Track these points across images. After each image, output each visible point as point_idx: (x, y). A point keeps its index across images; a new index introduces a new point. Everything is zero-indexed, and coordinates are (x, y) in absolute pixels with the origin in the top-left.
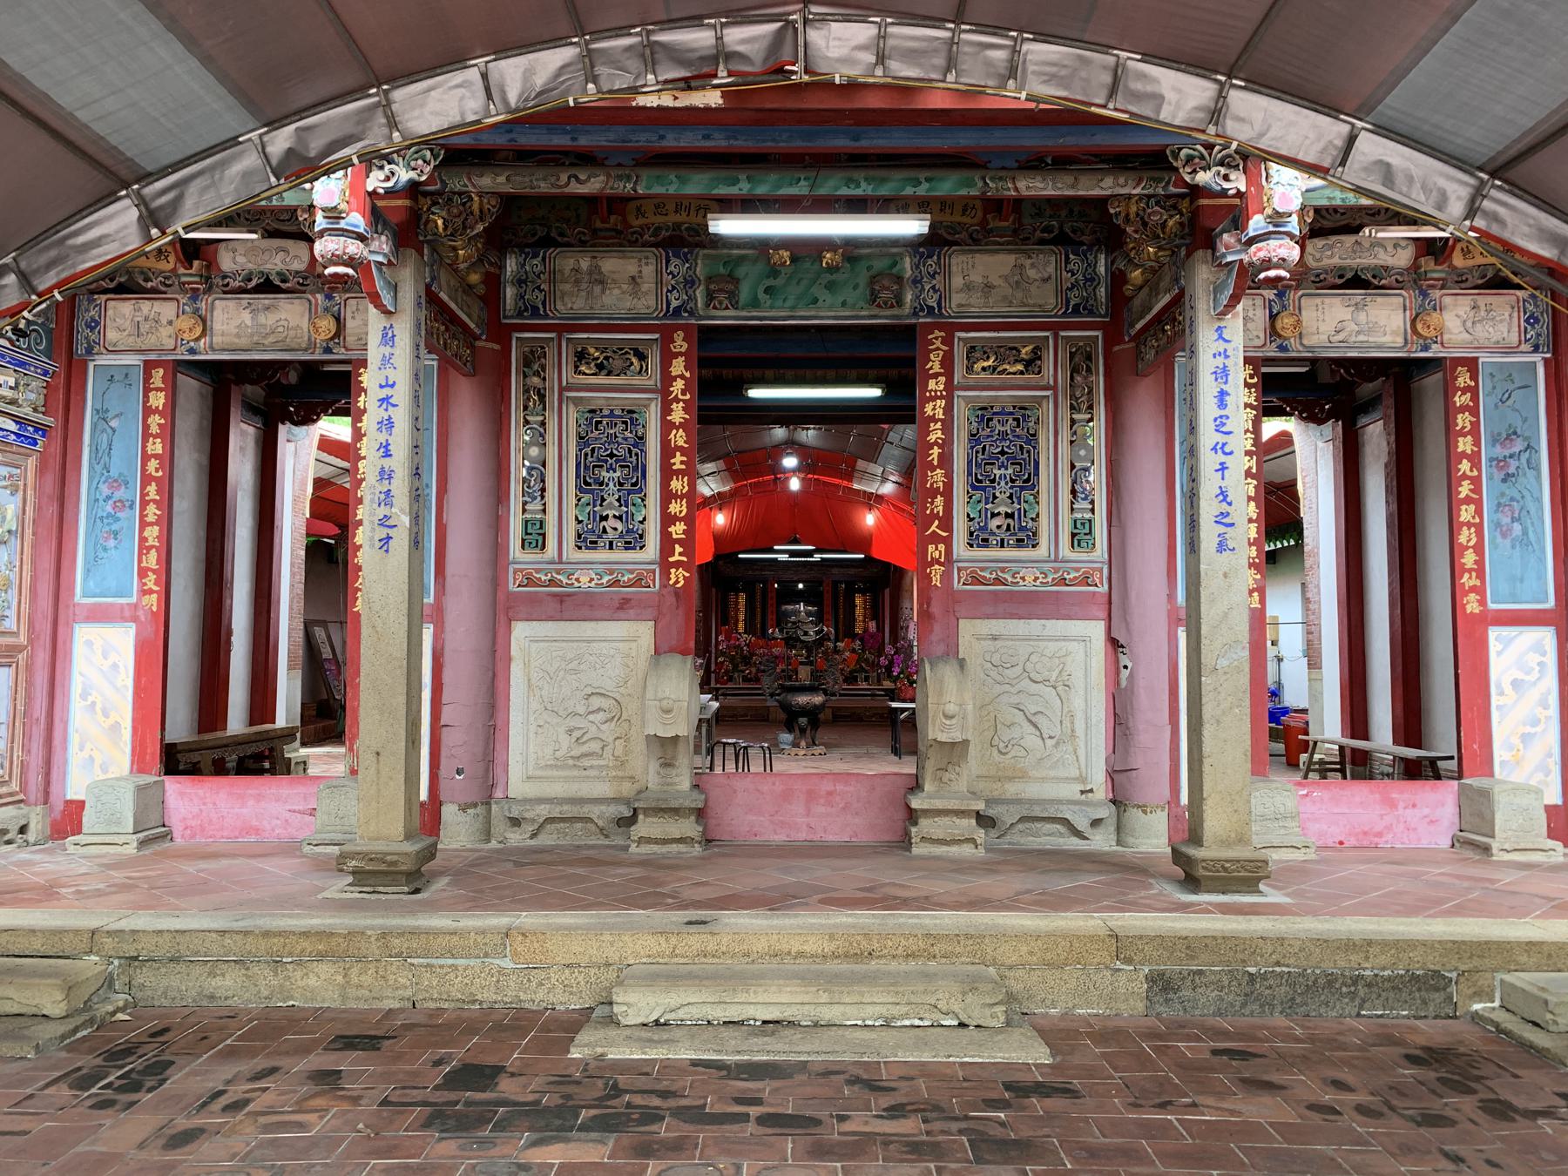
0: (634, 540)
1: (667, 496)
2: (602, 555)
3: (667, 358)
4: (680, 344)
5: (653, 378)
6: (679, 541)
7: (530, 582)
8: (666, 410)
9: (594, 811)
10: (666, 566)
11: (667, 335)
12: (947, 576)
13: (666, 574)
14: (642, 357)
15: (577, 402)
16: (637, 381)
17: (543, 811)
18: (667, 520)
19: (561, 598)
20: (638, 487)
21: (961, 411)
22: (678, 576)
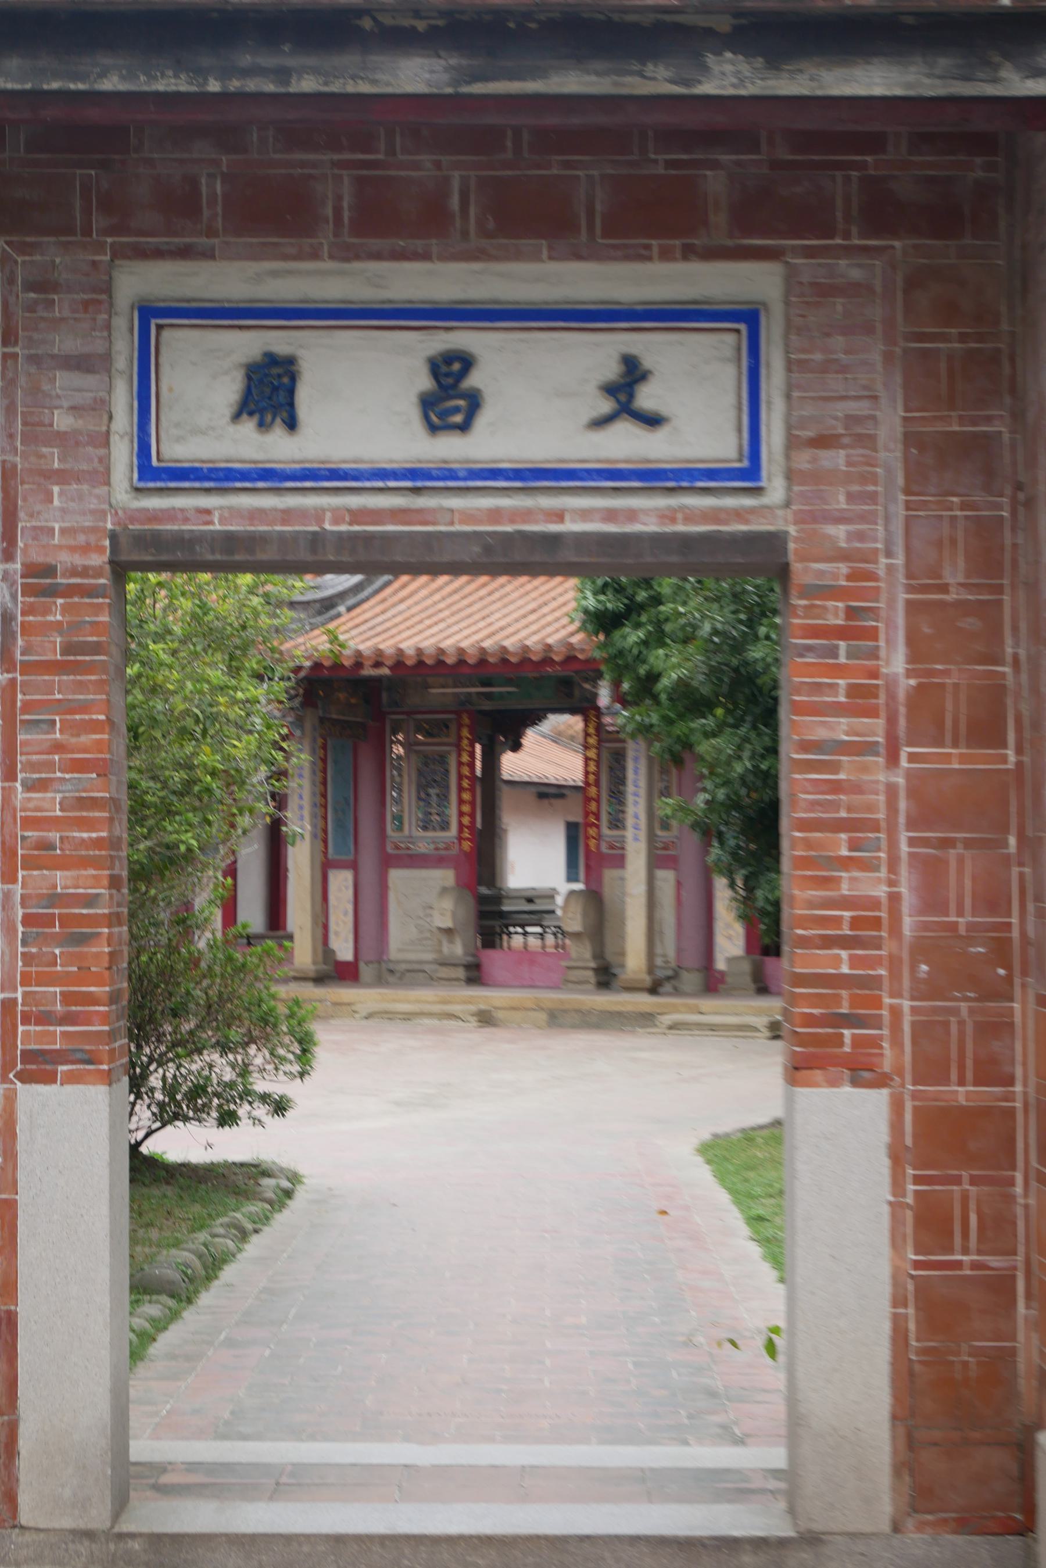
0: (445, 826)
1: (461, 802)
2: (430, 834)
3: (460, 726)
4: (466, 720)
5: (452, 739)
6: (467, 827)
7: (397, 848)
8: (459, 755)
9: (426, 967)
10: (460, 839)
11: (458, 713)
12: (598, 846)
13: (460, 844)
14: (447, 727)
15: (417, 752)
16: (445, 740)
17: (404, 966)
18: (461, 814)
19: (411, 856)
20: (444, 797)
21: (605, 755)
22: (467, 845)
